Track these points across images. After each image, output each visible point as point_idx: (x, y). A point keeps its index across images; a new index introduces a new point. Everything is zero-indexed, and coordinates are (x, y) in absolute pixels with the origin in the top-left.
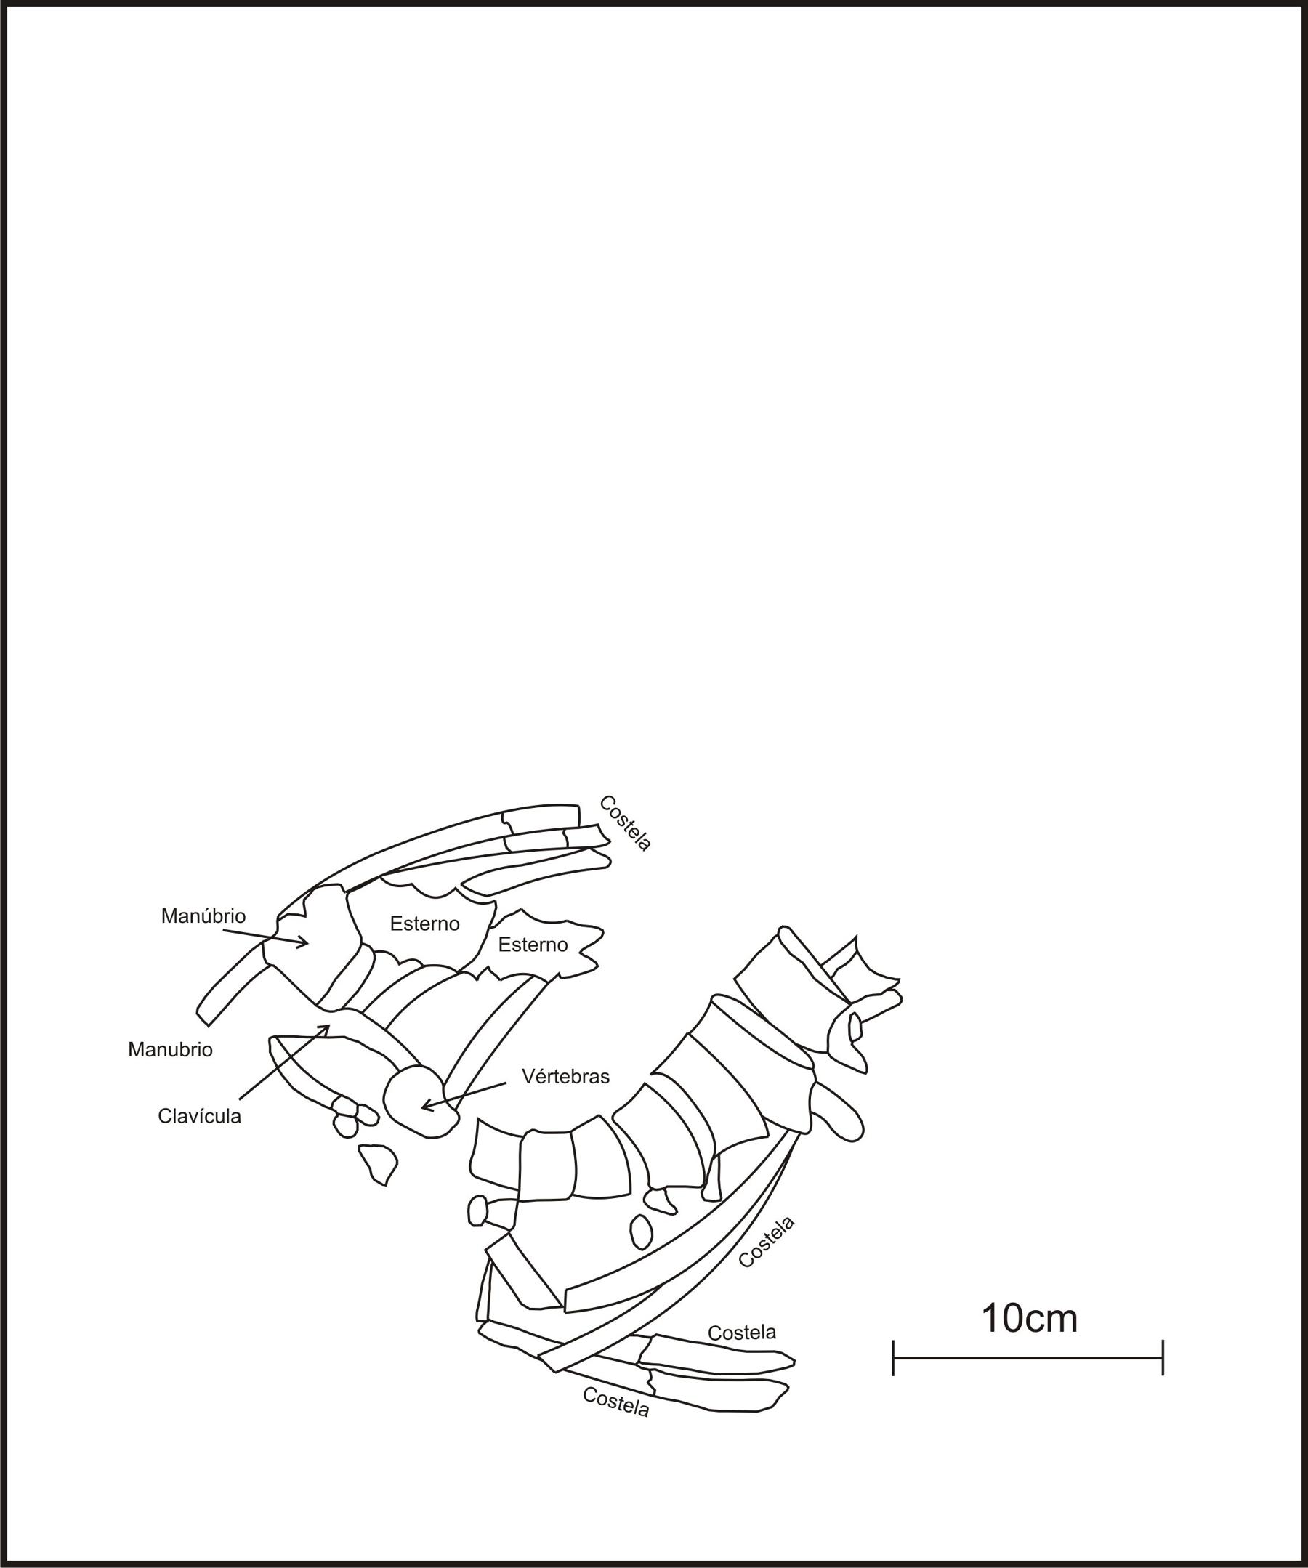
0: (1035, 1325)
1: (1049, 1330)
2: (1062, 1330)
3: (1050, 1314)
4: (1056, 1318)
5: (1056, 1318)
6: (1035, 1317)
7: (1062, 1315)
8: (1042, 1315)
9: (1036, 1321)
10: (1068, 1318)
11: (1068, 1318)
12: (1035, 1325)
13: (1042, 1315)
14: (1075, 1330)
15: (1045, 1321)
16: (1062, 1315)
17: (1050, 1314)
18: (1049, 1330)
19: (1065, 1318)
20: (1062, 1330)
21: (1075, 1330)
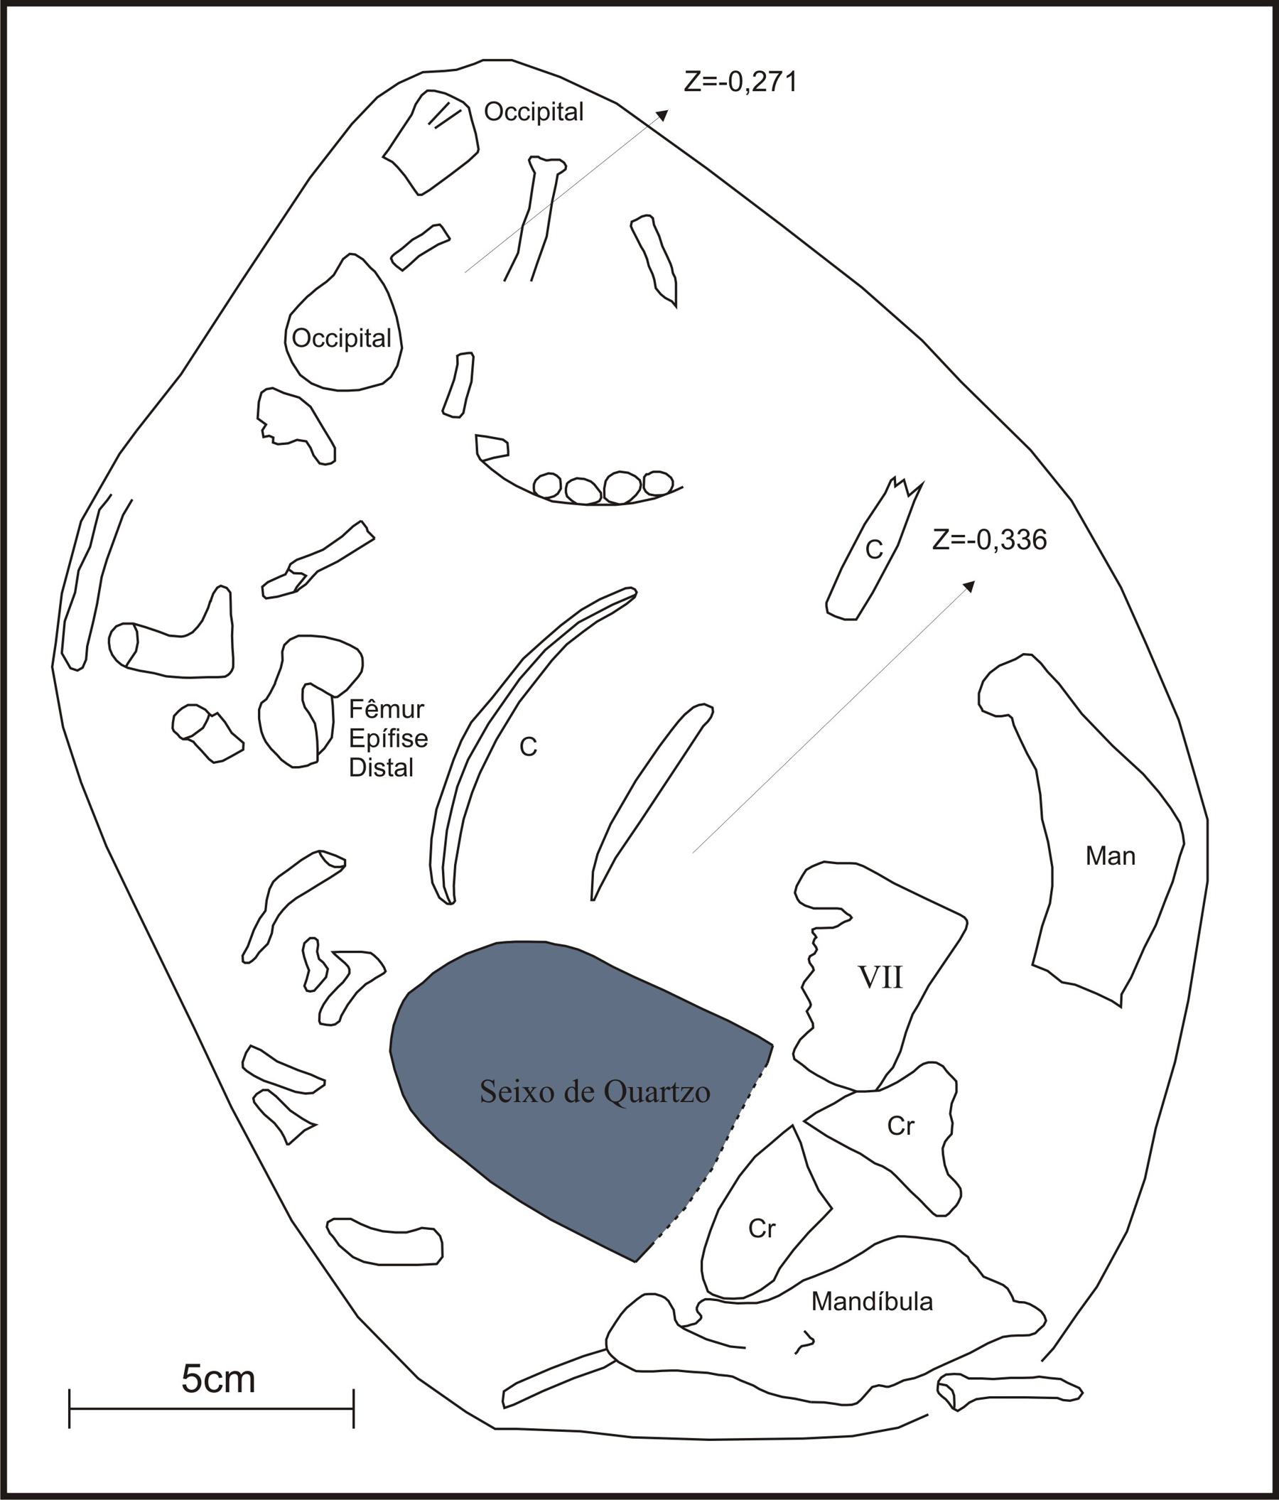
0: (214, 1387)
1: (228, 1390)
2: (240, 1390)
3: (228, 1375)
4: (234, 1378)
5: (234, 1378)
6: (213, 1378)
7: (240, 1376)
8: (220, 1376)
9: (214, 1382)
10: (246, 1378)
11: (246, 1378)
12: (214, 1387)
13: (220, 1376)
14: (252, 1390)
15: (223, 1381)
16: (240, 1376)
17: (228, 1375)
18: (228, 1390)
19: (243, 1378)
20: (240, 1390)
21: (252, 1390)
